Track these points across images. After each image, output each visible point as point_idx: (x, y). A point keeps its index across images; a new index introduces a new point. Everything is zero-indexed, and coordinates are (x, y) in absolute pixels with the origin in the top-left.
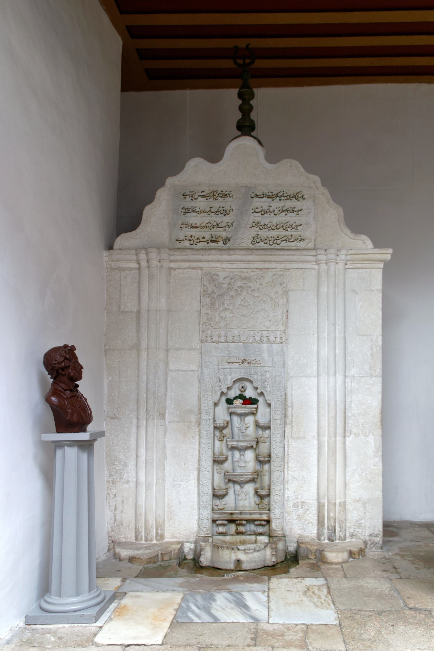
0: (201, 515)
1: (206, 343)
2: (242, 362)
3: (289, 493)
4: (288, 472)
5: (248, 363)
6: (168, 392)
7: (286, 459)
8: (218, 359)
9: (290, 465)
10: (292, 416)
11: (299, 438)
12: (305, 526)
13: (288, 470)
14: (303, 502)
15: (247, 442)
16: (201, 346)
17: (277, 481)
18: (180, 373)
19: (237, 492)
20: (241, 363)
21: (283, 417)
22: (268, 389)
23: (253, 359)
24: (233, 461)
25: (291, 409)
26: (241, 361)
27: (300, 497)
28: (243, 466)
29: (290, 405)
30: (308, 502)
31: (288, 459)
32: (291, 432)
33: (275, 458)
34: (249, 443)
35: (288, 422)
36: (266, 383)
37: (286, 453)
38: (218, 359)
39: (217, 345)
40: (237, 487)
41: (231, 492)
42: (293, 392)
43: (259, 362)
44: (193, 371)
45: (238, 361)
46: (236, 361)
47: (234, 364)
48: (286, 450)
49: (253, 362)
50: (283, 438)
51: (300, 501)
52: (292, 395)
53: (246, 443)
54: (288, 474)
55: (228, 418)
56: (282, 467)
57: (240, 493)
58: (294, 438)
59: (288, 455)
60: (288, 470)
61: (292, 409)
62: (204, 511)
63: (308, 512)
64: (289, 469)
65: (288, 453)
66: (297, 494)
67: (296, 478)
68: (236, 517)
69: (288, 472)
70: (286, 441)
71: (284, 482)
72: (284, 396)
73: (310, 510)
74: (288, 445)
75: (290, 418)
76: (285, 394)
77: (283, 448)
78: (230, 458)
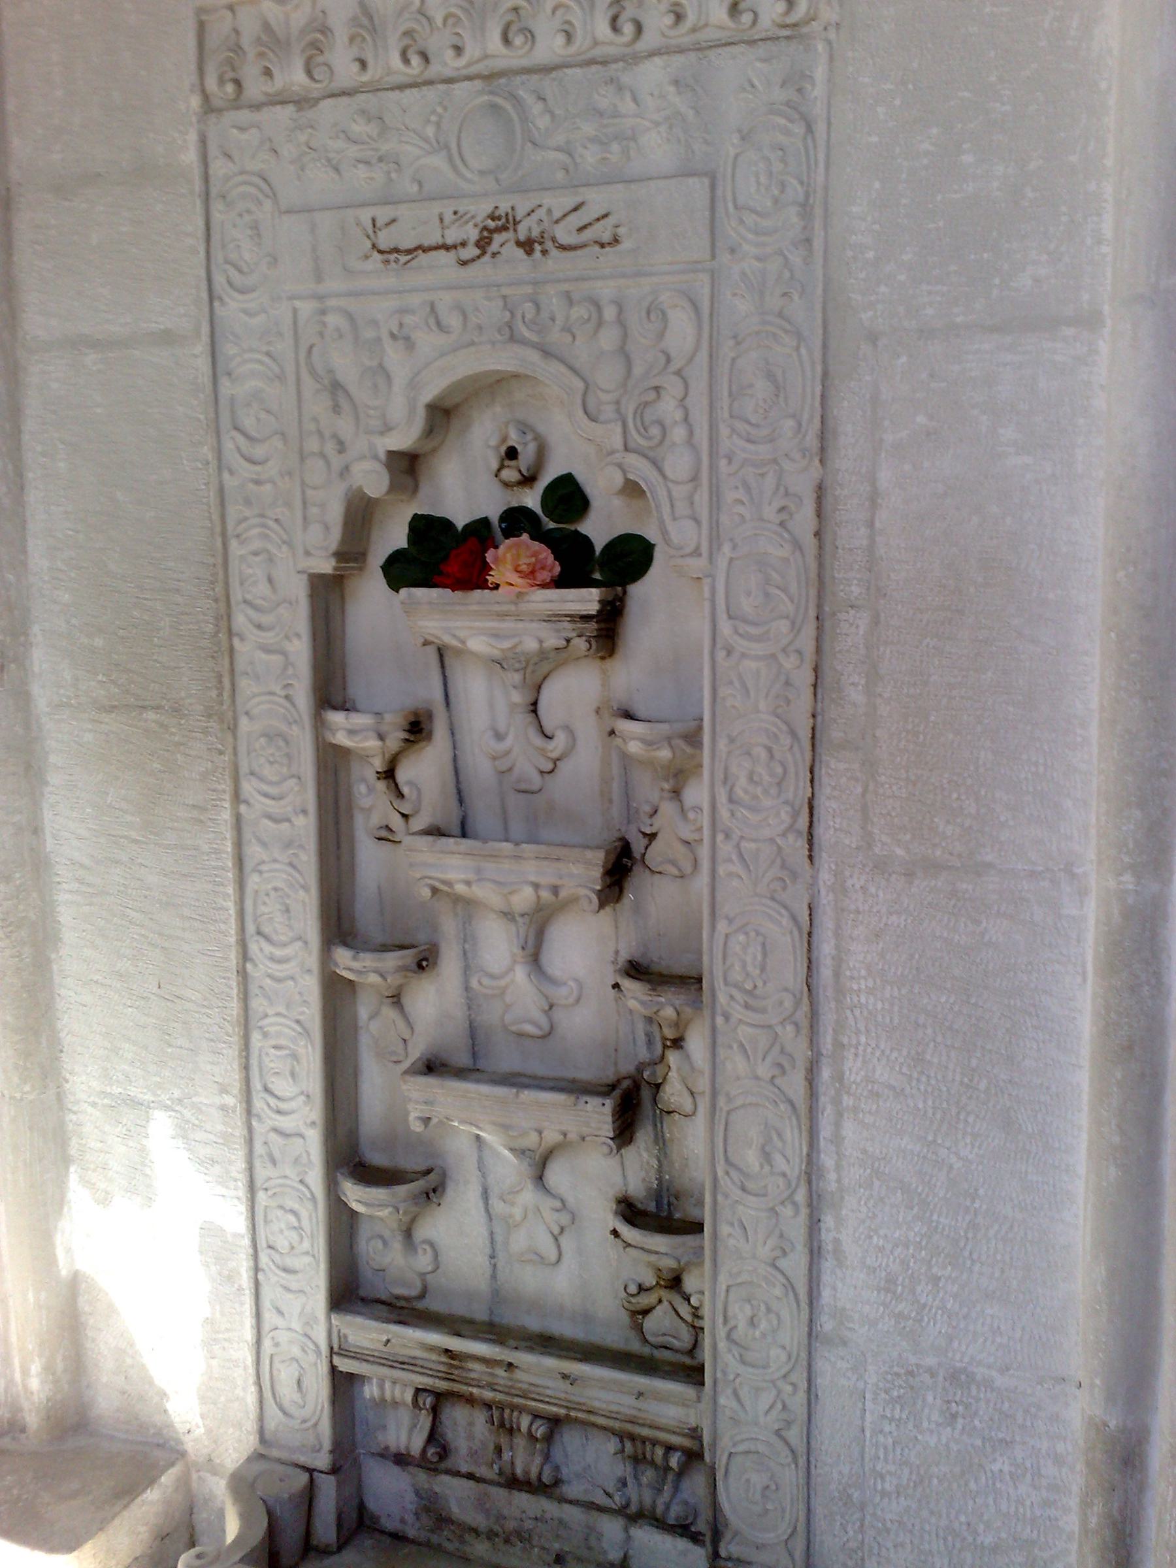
1: (231, 117)
2: (483, 244)
4: (838, 1125)
5: (527, 246)
6: (33, 496)
8: (313, 228)
9: (853, 1068)
11: (933, 867)
13: (839, 1114)
14: (958, 1377)
16: (203, 141)
18: (91, 358)
20: (471, 251)
23: (560, 202)
25: (863, 620)
26: (473, 234)
30: (1000, 1381)
31: (840, 1026)
33: (738, 1012)
38: (313, 228)
39: (310, 114)
42: (885, 477)
43: (603, 231)
44: (167, 338)
45: (452, 237)
46: (435, 238)
47: (423, 258)
48: (826, 949)
49: (564, 233)
51: (930, 1361)
52: (874, 500)
57: (517, 1212)
58: (881, 867)
59: (840, 991)
61: (876, 621)
63: (1001, 1464)
64: (847, 1101)
65: (837, 975)
72: (808, 510)
75: (856, 695)
76: (820, 491)
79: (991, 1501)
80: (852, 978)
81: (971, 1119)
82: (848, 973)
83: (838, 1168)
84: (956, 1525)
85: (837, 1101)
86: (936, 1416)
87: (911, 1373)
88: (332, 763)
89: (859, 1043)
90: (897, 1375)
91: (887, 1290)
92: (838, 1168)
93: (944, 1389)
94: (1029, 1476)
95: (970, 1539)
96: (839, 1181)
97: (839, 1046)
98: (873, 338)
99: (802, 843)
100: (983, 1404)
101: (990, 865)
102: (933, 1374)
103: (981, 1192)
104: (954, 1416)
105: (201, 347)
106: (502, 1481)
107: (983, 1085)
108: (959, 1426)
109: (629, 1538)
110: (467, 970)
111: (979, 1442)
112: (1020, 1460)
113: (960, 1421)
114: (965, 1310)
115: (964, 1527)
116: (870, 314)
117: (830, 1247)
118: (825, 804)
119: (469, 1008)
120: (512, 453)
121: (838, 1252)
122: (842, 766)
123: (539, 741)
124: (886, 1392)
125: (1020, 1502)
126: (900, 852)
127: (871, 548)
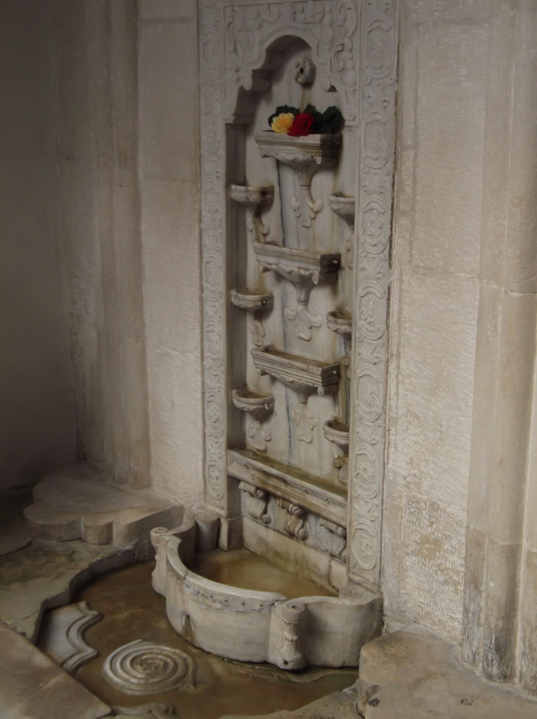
0: (207, 453)
3: (399, 463)
4: (397, 387)
7: (394, 340)
10: (415, 182)
12: (435, 585)
15: (300, 261)
17: (368, 409)
19: (292, 413)
21: (388, 186)
22: (350, 76)
24: (283, 316)
27: (425, 484)
28: (302, 335)
29: (408, 141)
30: (449, 510)
32: (411, 244)
34: (303, 265)
35: (402, 207)
36: (346, 55)
37: (394, 321)
40: (294, 398)
41: (279, 407)
48: (394, 308)
50: (386, 264)
51: (425, 497)
53: (297, 264)
54: (397, 394)
55: (272, 178)
56: (382, 366)
59: (400, 327)
60: (398, 383)
61: (416, 156)
62: (214, 445)
64: (401, 378)
65: (399, 319)
66: (416, 472)
67: (417, 417)
68: (275, 487)
69: (397, 387)
70: (396, 275)
71: (384, 419)
72: (393, 102)
73: (454, 542)
74: (401, 290)
75: (409, 190)
77: (384, 301)
78: (277, 305)
79: (443, 562)
80: (404, 321)
81: (441, 389)
82: (403, 319)
83: (397, 406)
84: (431, 571)
85: (397, 377)
86: (426, 521)
87: (417, 502)
88: (235, 209)
89: (405, 352)
90: (413, 502)
91: (411, 463)
92: (397, 406)
93: (429, 510)
94: (456, 552)
95: (436, 577)
96: (397, 413)
97: (399, 353)
98: (418, 25)
99: (387, 258)
100: (442, 518)
101: (452, 273)
102: (426, 504)
103: (444, 423)
104: (432, 523)
105: (195, 24)
106: (285, 532)
107: (445, 374)
108: (434, 527)
109: (330, 566)
110: (283, 307)
111: (440, 535)
112: (454, 545)
113: (434, 525)
114: (436, 476)
115: (434, 572)
116: (416, 15)
117: (393, 442)
118: (397, 240)
119: (284, 325)
120: (302, 71)
121: (395, 444)
122: (404, 222)
123: (310, 204)
124: (409, 509)
125: (453, 564)
126: (421, 264)
127: (415, 123)
